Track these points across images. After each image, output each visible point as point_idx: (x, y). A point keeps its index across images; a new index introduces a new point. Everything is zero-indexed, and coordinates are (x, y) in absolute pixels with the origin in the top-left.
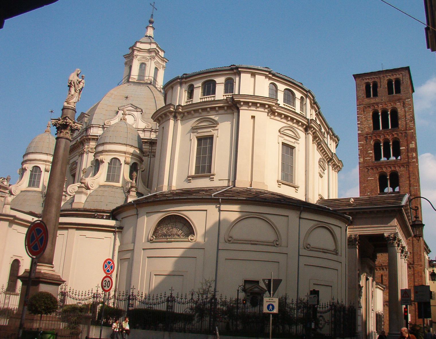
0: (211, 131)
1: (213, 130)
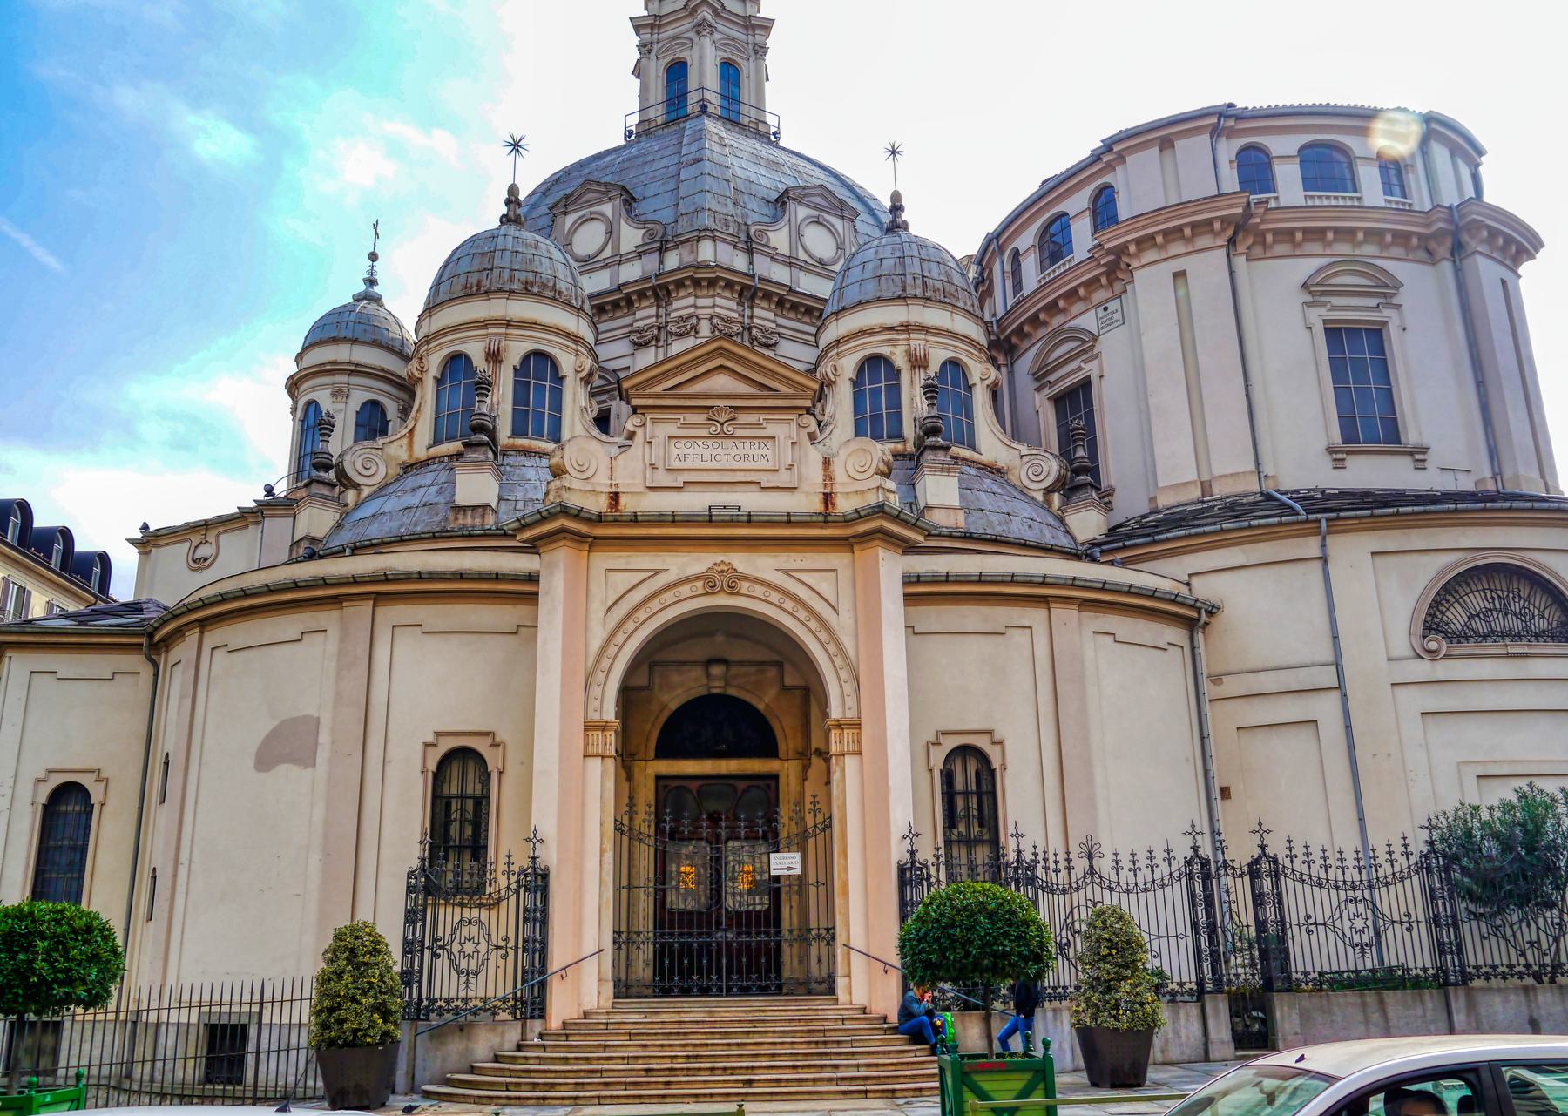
0: (1080, 369)
1: (1086, 361)
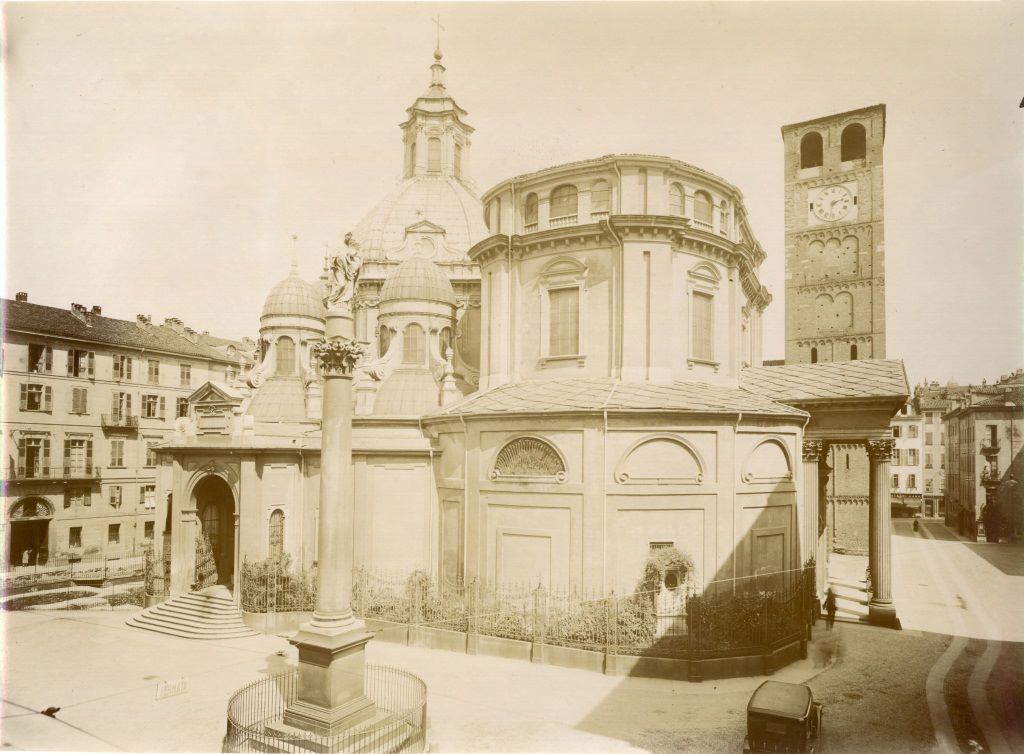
1: (578, 279)
